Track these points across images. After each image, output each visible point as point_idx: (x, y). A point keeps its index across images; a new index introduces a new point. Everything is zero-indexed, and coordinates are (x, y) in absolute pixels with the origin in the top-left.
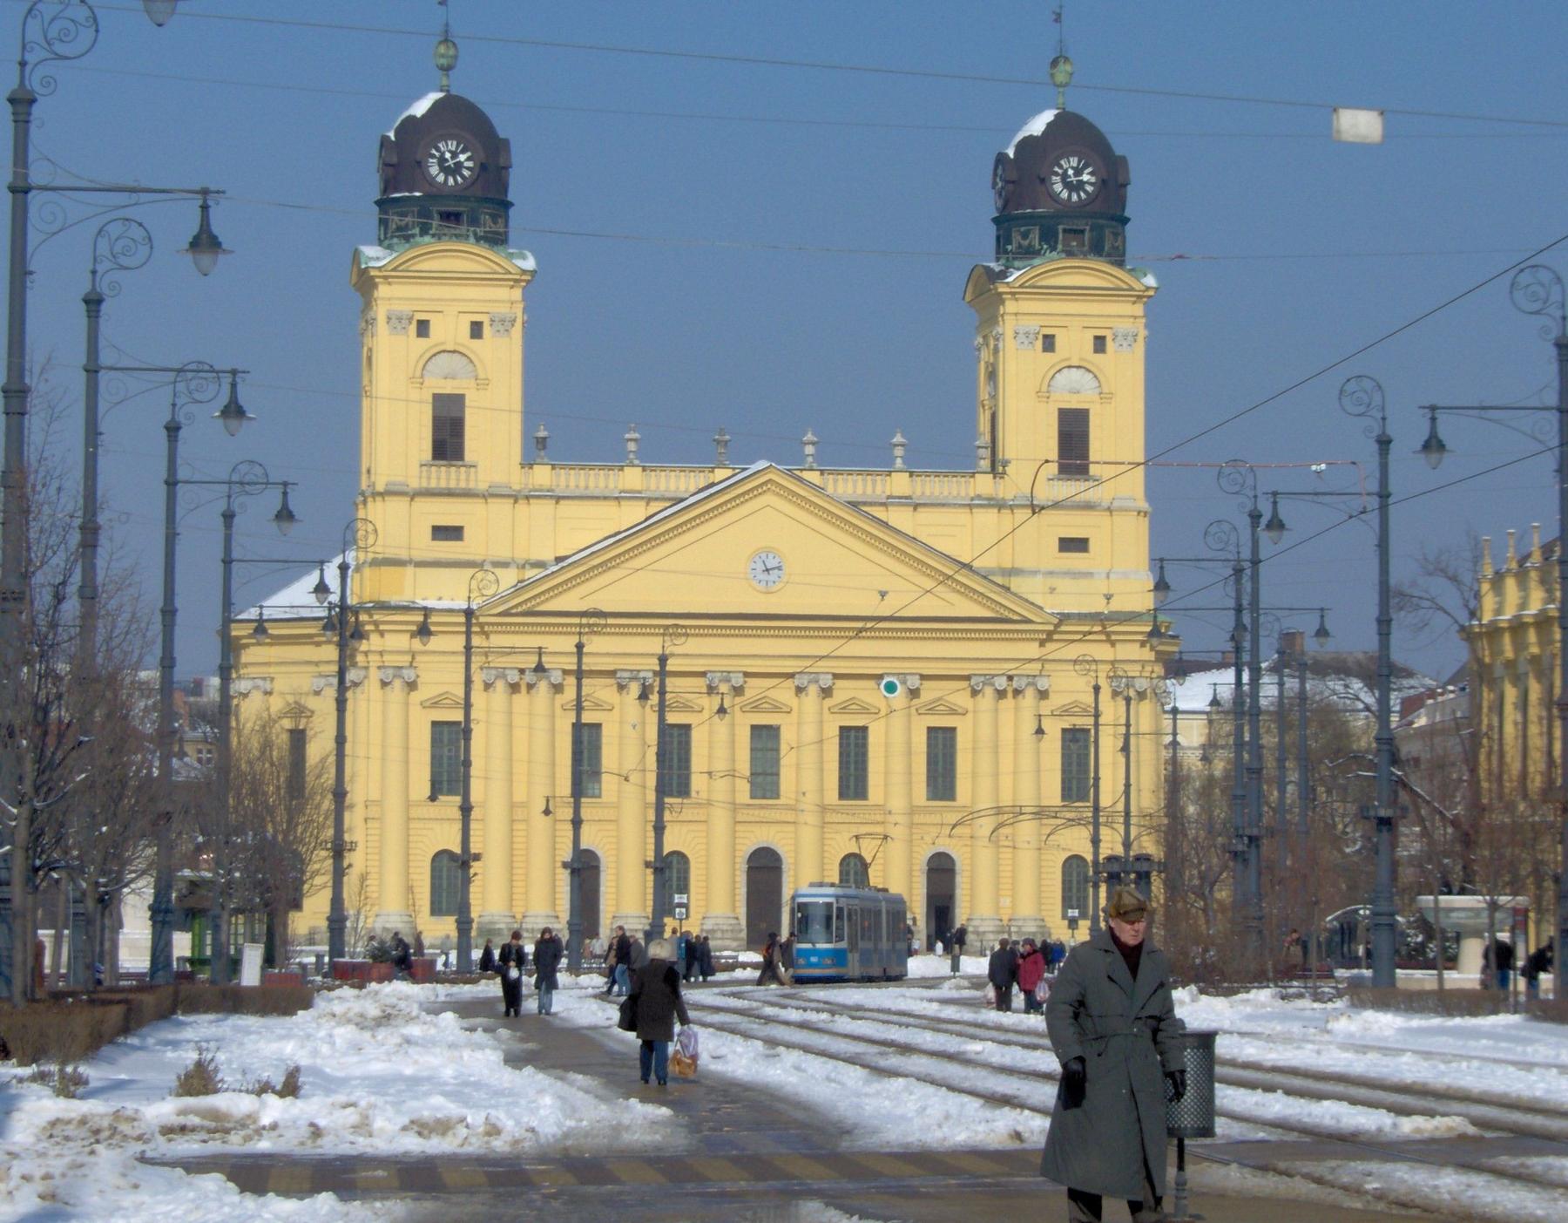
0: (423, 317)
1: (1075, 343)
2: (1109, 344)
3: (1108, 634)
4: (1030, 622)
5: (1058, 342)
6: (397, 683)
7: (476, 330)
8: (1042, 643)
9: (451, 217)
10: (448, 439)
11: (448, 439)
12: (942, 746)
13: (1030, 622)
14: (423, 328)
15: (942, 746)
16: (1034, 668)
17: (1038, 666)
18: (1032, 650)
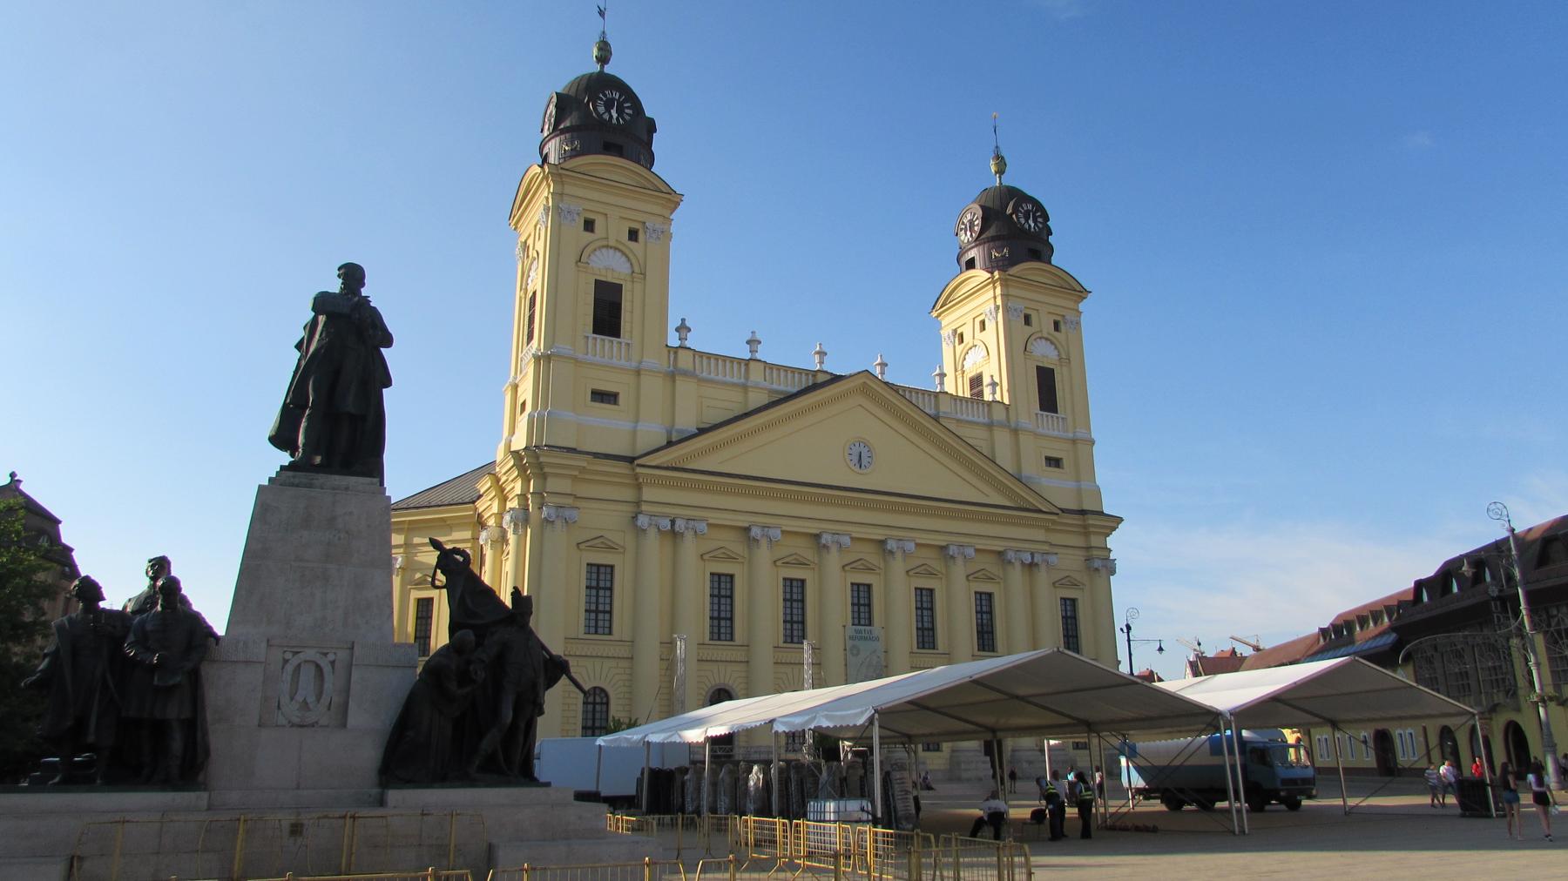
0: (591, 216)
1: (1043, 323)
2: (1062, 327)
3: (1085, 527)
4: (1040, 511)
5: (1034, 319)
6: (559, 523)
7: (633, 235)
8: (1048, 530)
9: (610, 148)
10: (607, 318)
11: (607, 318)
12: (985, 604)
13: (1040, 511)
14: (589, 225)
15: (985, 604)
16: (1046, 548)
17: (1046, 548)
18: (1040, 535)
